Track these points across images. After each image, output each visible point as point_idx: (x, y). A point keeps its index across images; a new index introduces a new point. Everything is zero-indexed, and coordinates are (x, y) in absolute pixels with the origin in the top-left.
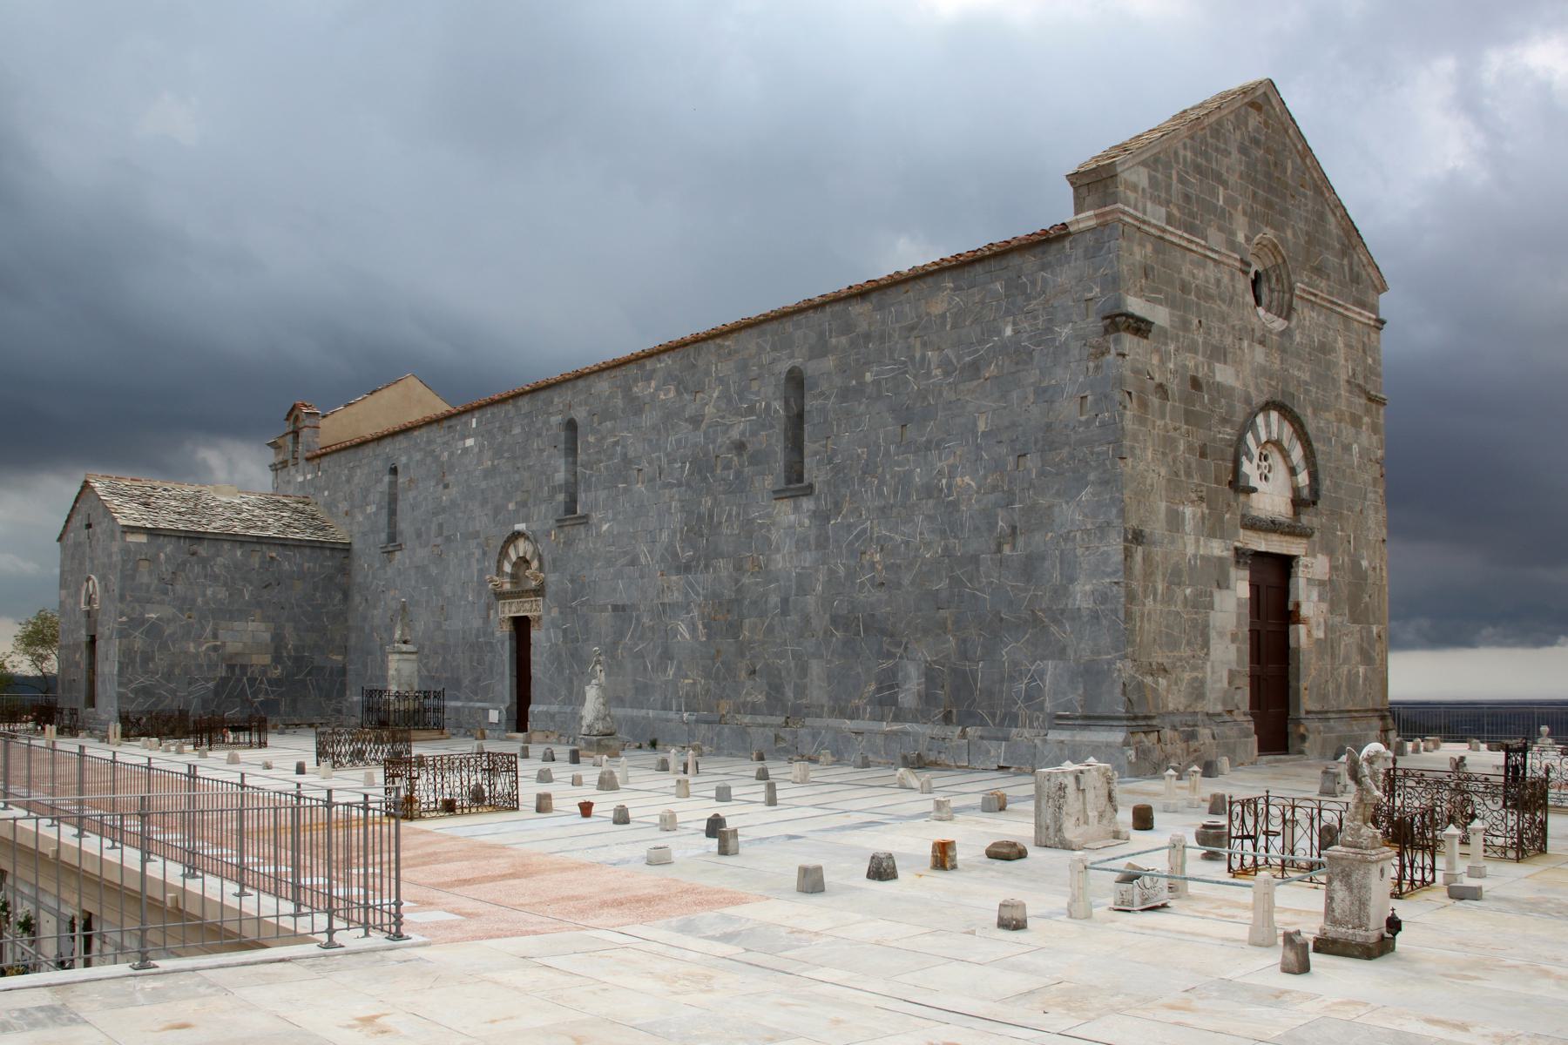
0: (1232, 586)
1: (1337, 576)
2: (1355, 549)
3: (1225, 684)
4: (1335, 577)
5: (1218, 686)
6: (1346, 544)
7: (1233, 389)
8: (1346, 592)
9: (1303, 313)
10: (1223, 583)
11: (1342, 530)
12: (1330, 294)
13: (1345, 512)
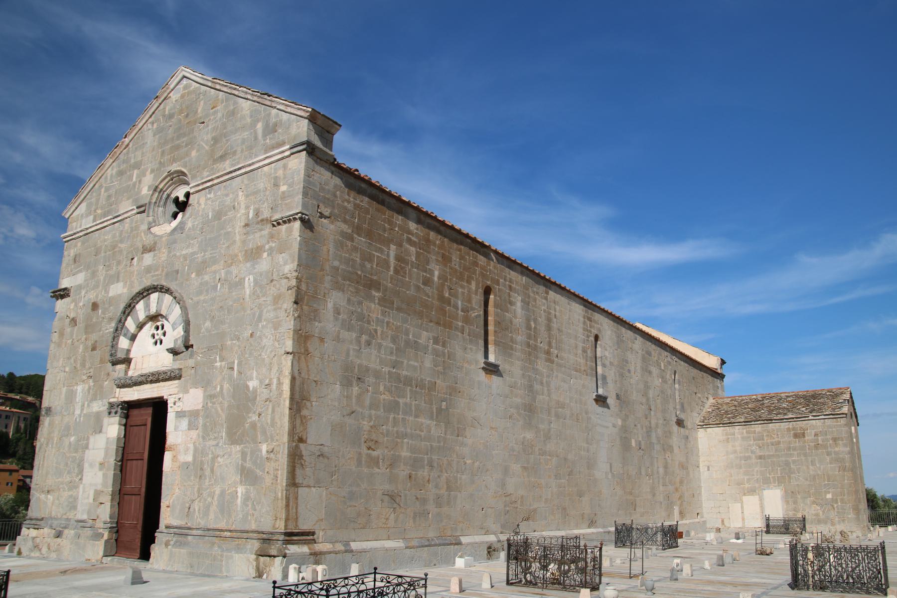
0: (104, 430)
1: (214, 403)
2: (240, 373)
3: (91, 500)
4: (210, 405)
5: (86, 501)
6: (226, 371)
8: (224, 416)
10: (99, 429)
11: (222, 360)
12: (233, 165)
13: (229, 343)
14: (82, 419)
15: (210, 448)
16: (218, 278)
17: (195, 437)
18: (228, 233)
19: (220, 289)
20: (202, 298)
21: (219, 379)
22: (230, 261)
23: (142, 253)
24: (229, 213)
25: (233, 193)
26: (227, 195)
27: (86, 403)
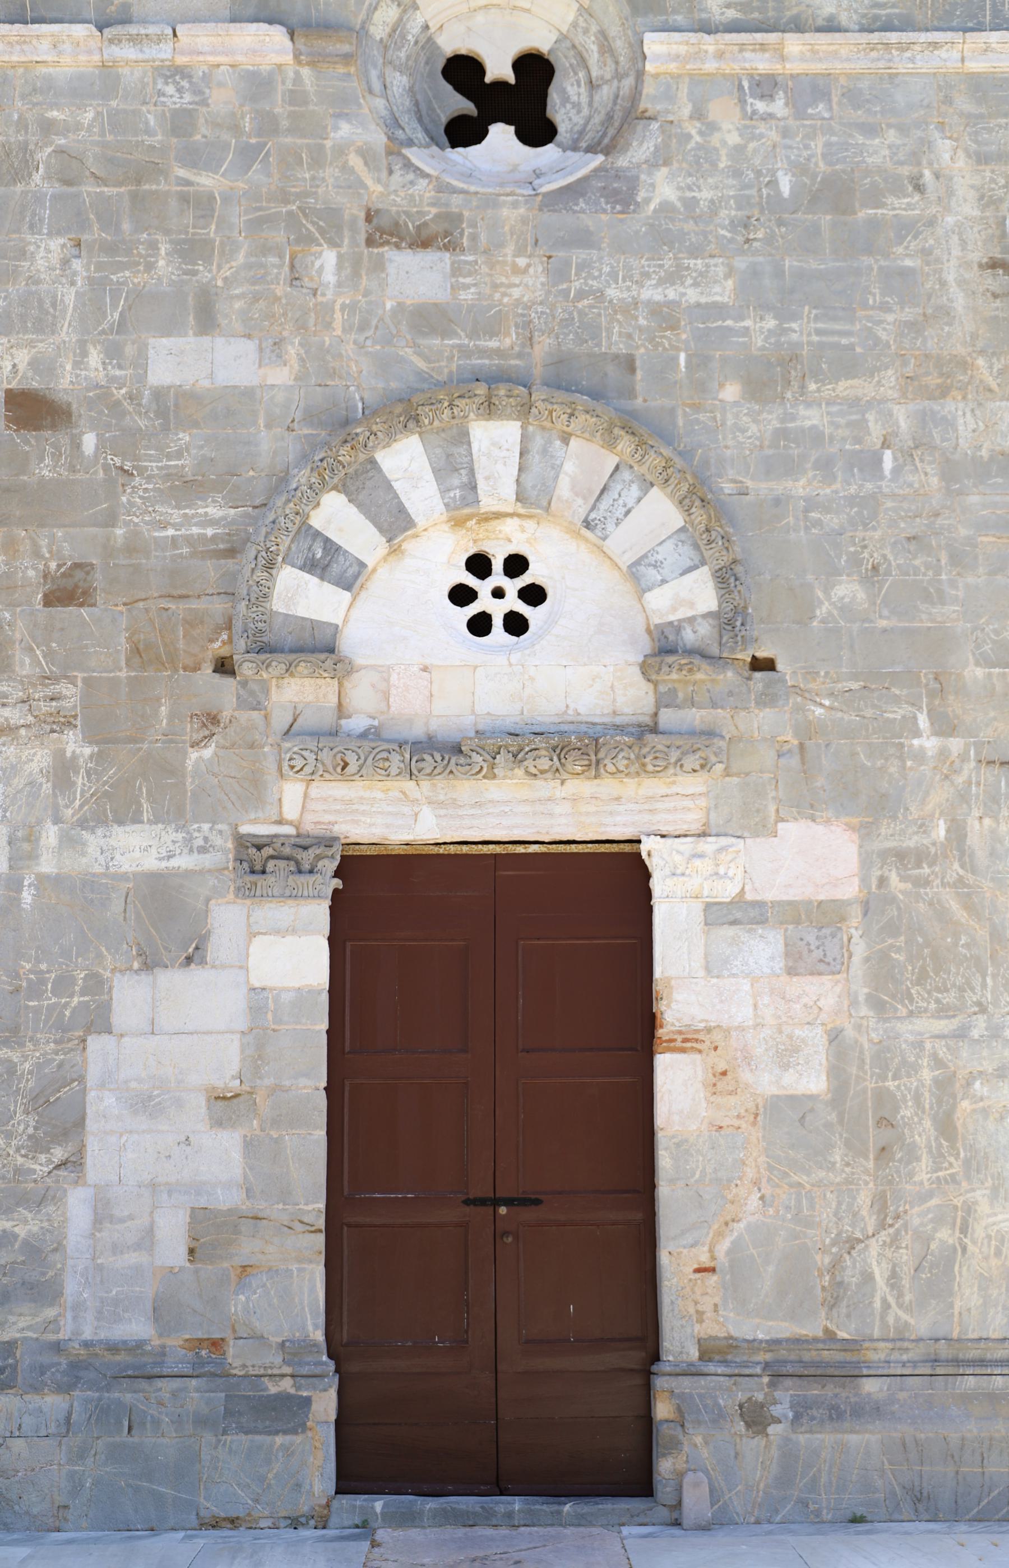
7: (248, 394)
9: (698, 114)
14: (27, 897)
15: (919, 1045)
16: (876, 431)
17: (829, 1002)
18: (905, 273)
19: (896, 471)
20: (800, 487)
21: (939, 796)
22: (933, 381)
23: (370, 242)
24: (890, 200)
25: (903, 130)
26: (871, 130)
27: (50, 835)
